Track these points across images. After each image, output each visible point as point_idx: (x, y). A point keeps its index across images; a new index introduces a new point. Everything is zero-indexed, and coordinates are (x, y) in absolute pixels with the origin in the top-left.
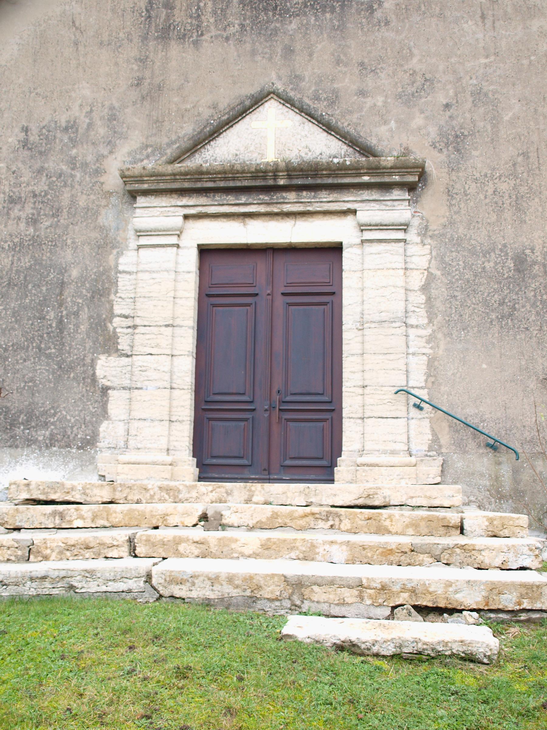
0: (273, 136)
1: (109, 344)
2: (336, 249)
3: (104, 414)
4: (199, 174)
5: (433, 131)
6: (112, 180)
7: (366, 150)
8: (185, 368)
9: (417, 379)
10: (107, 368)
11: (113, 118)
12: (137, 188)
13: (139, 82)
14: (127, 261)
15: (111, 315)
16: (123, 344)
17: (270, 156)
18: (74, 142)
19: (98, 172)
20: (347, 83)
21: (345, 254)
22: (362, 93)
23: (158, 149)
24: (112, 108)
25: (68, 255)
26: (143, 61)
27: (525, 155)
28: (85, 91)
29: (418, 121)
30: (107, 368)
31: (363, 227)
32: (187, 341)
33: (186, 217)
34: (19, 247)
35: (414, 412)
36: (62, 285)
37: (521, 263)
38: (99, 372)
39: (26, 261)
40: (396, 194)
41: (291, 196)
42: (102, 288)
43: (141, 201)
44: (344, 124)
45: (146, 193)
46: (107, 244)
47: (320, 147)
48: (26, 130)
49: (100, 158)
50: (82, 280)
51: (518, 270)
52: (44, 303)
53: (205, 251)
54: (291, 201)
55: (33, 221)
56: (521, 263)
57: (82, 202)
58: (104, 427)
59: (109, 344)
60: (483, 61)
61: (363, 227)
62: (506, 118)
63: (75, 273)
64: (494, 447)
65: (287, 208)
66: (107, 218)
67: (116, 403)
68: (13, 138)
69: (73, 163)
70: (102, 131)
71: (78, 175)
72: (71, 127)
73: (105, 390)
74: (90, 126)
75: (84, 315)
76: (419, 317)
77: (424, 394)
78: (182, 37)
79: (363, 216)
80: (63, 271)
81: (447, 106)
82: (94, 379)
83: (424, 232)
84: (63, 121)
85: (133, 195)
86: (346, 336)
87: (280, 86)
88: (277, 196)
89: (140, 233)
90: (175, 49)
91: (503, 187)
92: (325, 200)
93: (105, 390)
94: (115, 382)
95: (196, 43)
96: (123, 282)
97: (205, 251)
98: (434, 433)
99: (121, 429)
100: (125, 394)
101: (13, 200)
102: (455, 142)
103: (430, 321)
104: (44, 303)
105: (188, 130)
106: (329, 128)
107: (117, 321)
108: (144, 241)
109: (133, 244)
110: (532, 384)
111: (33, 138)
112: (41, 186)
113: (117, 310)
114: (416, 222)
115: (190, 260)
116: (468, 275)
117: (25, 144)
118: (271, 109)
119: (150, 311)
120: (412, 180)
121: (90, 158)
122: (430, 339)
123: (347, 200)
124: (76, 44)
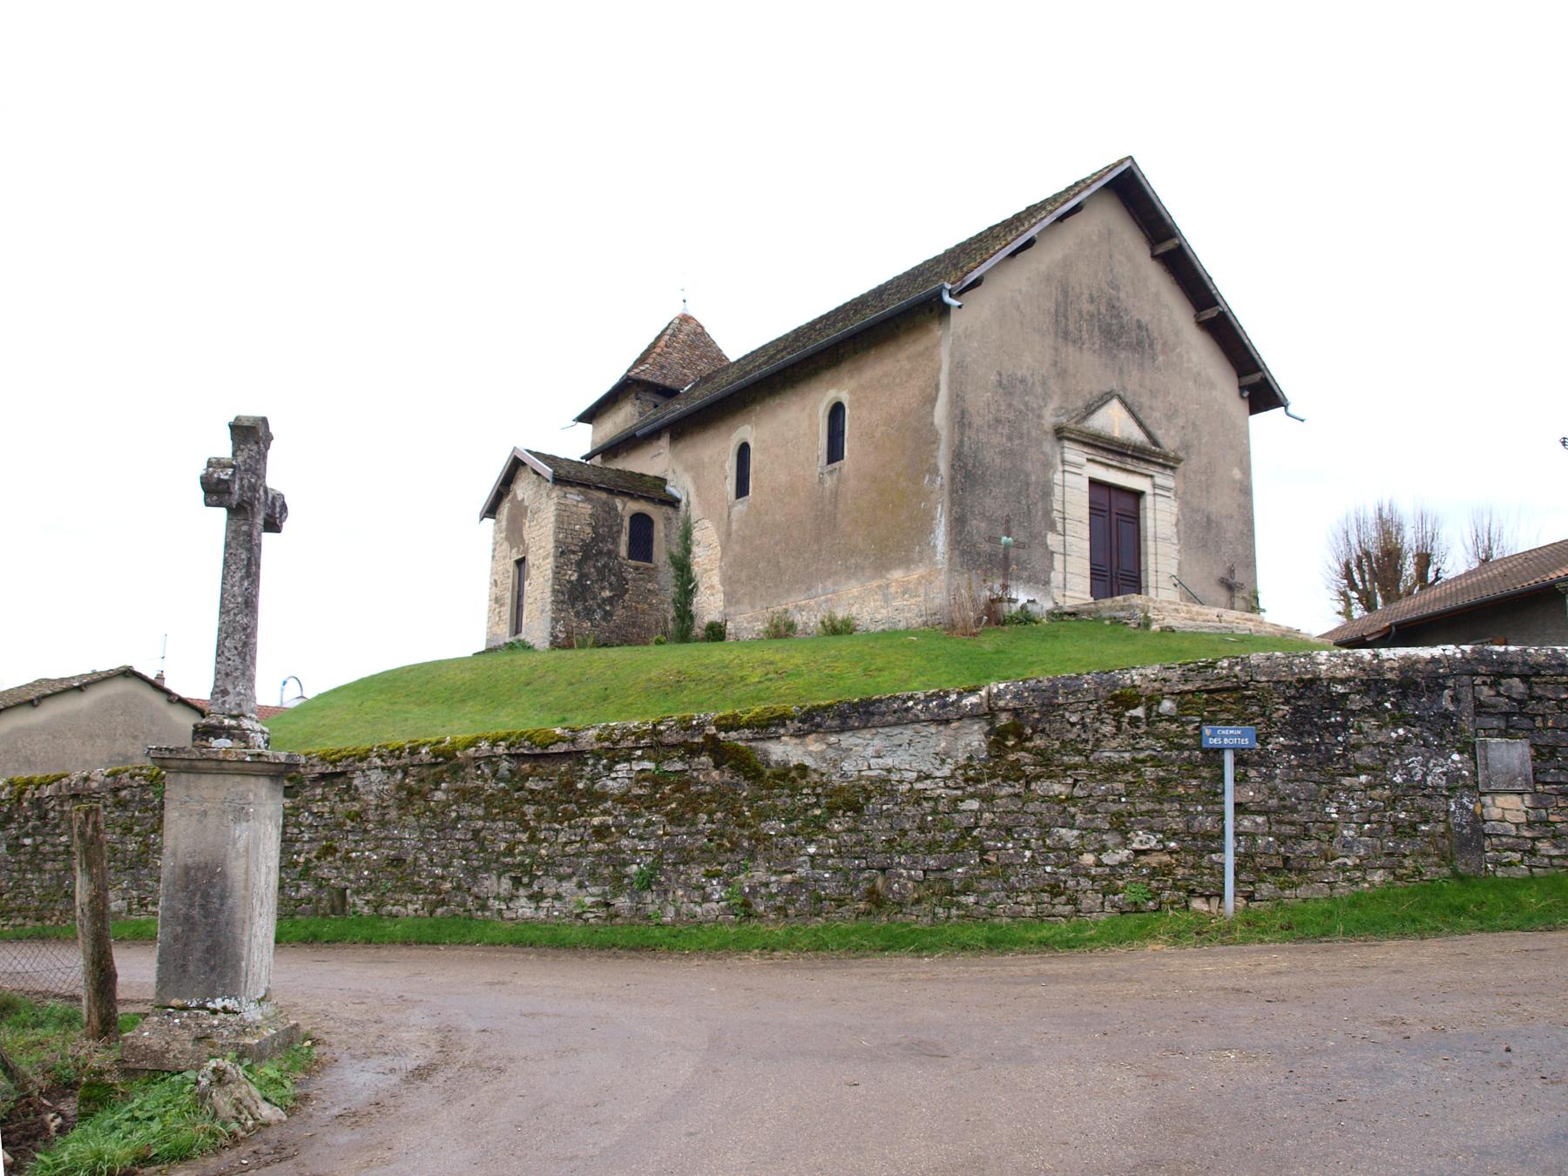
1: (1052, 526)
2: (1138, 495)
7: (1155, 443)
11: (1044, 383)
16: (1059, 527)
18: (1026, 393)
23: (1067, 411)
25: (1029, 467)
26: (1056, 349)
30: (1053, 540)
34: (1003, 453)
39: (1008, 465)
42: (1047, 493)
44: (1147, 423)
45: (1069, 439)
46: (1047, 466)
47: (1138, 436)
48: (1000, 374)
49: (1040, 408)
50: (1037, 483)
54: (1130, 464)
59: (1052, 526)
61: (1155, 486)
67: (1058, 561)
68: (994, 378)
75: (1040, 505)
78: (1074, 342)
80: (1027, 475)
82: (1047, 547)
90: (1071, 349)
92: (1142, 467)
96: (1057, 490)
99: (1061, 577)
101: (998, 421)
106: (1141, 425)
111: (1004, 381)
112: (1012, 417)
113: (1055, 506)
118: (1115, 403)
119: (1071, 511)
123: (1152, 470)
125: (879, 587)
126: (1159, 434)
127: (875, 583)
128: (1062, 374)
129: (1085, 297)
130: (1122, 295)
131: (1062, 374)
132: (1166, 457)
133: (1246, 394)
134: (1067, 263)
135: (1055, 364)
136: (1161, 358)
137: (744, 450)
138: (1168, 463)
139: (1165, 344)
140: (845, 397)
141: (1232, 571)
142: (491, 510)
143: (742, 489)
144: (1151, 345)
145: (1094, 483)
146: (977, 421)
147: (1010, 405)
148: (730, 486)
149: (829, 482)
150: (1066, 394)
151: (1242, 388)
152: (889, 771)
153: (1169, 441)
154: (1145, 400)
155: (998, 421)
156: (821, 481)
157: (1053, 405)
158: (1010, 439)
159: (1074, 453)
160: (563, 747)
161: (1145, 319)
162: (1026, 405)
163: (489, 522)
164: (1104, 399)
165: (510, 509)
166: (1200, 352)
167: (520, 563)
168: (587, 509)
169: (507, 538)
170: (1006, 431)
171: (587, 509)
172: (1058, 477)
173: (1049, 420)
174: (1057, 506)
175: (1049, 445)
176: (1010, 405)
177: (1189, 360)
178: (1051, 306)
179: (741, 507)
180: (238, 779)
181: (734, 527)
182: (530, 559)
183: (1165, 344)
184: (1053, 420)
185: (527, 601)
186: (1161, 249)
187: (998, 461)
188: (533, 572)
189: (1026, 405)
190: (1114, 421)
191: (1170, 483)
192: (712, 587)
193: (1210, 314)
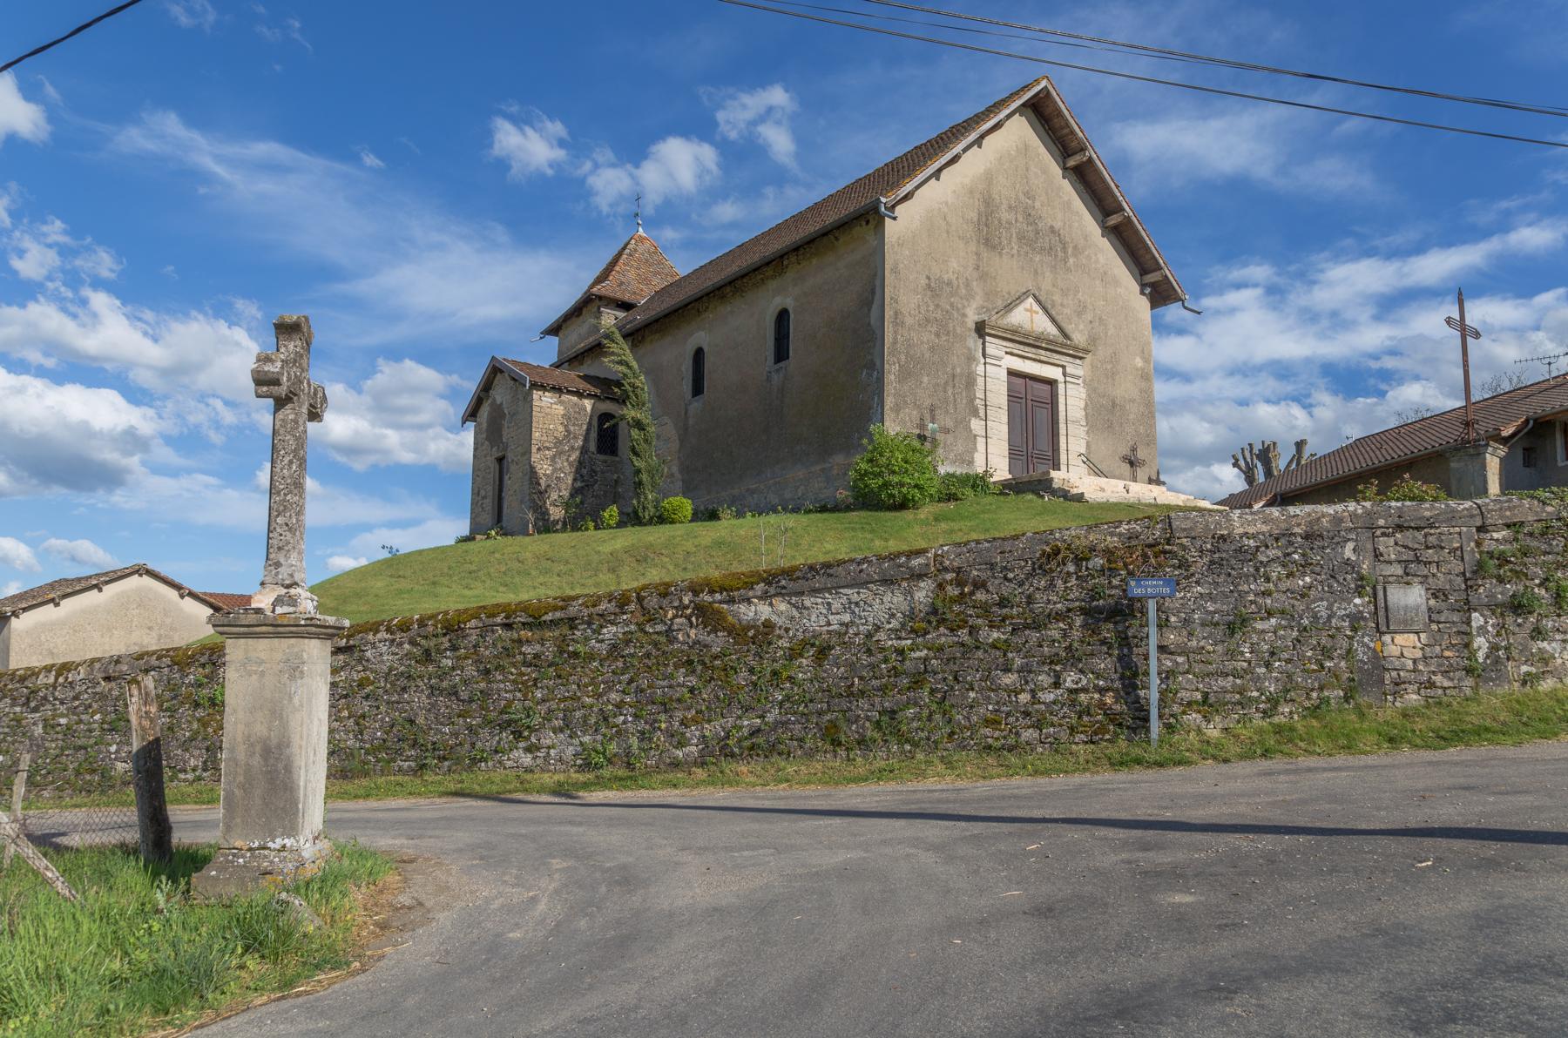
1: (975, 413)
2: (1052, 383)
7: (1066, 336)
11: (967, 285)
16: (982, 413)
18: (952, 294)
30: (976, 425)
42: (970, 382)
46: (971, 359)
59: (975, 413)
61: (1065, 374)
67: (981, 442)
68: (923, 282)
96: (980, 381)
106: (1053, 320)
112: (939, 316)
123: (1063, 360)
125: (823, 470)
126: (1069, 328)
127: (818, 468)
128: (983, 277)
129: (1004, 207)
130: (1037, 204)
131: (983, 277)
132: (1076, 348)
133: (1148, 291)
134: (989, 178)
135: (977, 268)
137: (699, 355)
138: (1078, 354)
139: (1075, 247)
140: (789, 303)
141: (1134, 450)
142: (472, 414)
143: (698, 389)
144: (1064, 249)
145: (1012, 373)
146: (909, 321)
147: (937, 306)
148: (687, 386)
149: (776, 379)
150: (987, 295)
151: (1143, 286)
152: (847, 625)
154: (1057, 298)
155: (928, 321)
156: (769, 379)
158: (938, 335)
159: (994, 347)
160: (558, 615)
161: (1058, 225)
162: (952, 305)
163: (471, 425)
164: (1019, 299)
165: (490, 413)
166: (1106, 254)
167: (500, 460)
168: (560, 409)
169: (487, 439)
170: (934, 329)
171: (560, 409)
172: (980, 369)
173: (972, 317)
174: (980, 394)
175: (973, 342)
176: (937, 306)
177: (1097, 261)
178: (974, 215)
179: (696, 405)
180: (293, 641)
181: (691, 422)
182: (510, 456)
183: (1075, 247)
184: (976, 318)
185: (506, 494)
186: (1071, 163)
187: (927, 355)
188: (513, 468)
189: (952, 305)
190: (1026, 316)
191: (1080, 372)
192: (672, 475)
193: (1114, 220)
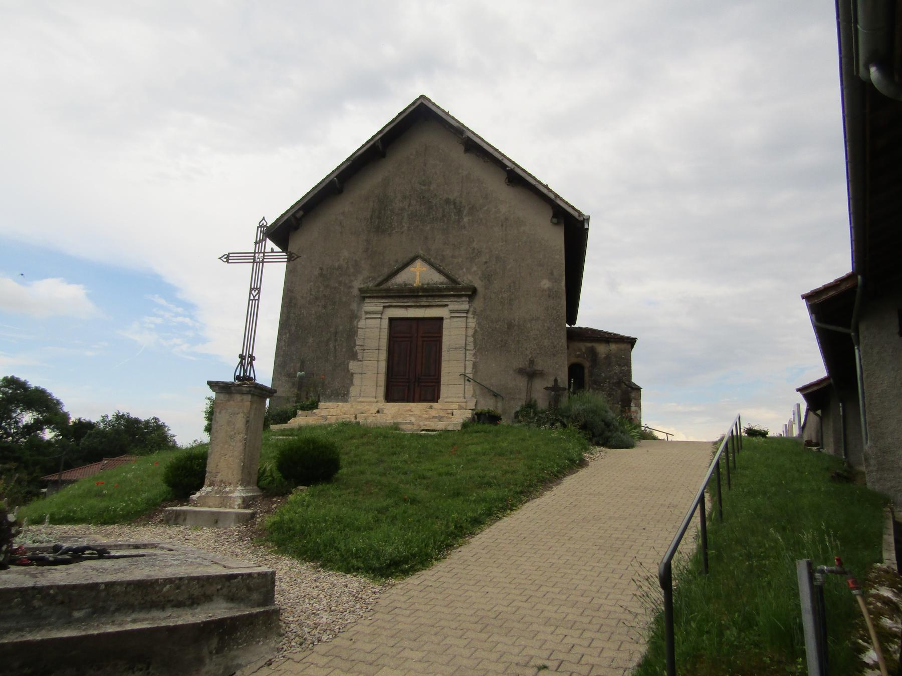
0: (419, 274)
1: (354, 356)
2: (441, 319)
3: (352, 383)
4: (388, 290)
5: (480, 273)
6: (355, 292)
7: (454, 281)
8: (383, 365)
9: (469, 370)
10: (353, 366)
12: (365, 295)
13: (366, 250)
14: (362, 324)
15: (355, 345)
16: (360, 357)
17: (417, 283)
19: (351, 287)
20: (448, 252)
21: (445, 322)
22: (453, 257)
24: (356, 261)
27: (514, 283)
28: (346, 253)
29: (475, 269)
30: (353, 366)
31: (452, 311)
32: (383, 356)
33: (384, 307)
35: (467, 382)
36: (336, 333)
37: (510, 326)
38: (350, 367)
40: (464, 299)
41: (424, 299)
42: (352, 333)
43: (367, 300)
45: (369, 297)
46: (354, 317)
47: (436, 278)
48: (321, 269)
49: (351, 281)
51: (508, 328)
52: (329, 340)
53: (391, 320)
55: (325, 307)
56: (510, 326)
57: (344, 299)
58: (352, 389)
59: (354, 356)
60: (501, 244)
61: (452, 311)
62: (508, 268)
63: (341, 328)
64: (496, 395)
65: (423, 304)
66: (354, 306)
67: (357, 380)
68: (316, 272)
69: (340, 283)
70: (352, 270)
71: (342, 288)
72: (340, 267)
73: (352, 374)
74: (348, 268)
76: (471, 346)
77: (471, 376)
79: (451, 307)
81: (486, 262)
82: (348, 370)
83: (474, 313)
84: (336, 265)
85: (364, 298)
86: (443, 354)
87: (421, 252)
88: (419, 300)
89: (367, 313)
91: (505, 295)
92: (438, 301)
93: (352, 374)
94: (356, 371)
95: (390, 235)
96: (360, 332)
97: (391, 320)
98: (474, 390)
100: (360, 376)
102: (488, 278)
103: (475, 348)
104: (329, 340)
105: (386, 271)
106: (440, 271)
107: (357, 347)
108: (368, 316)
109: (364, 317)
110: (511, 372)
113: (358, 343)
114: (472, 309)
115: (385, 323)
116: (490, 330)
117: (321, 275)
120: (472, 293)
121: (347, 282)
122: (475, 354)
123: (445, 301)
124: (341, 233)
136: (466, 220)
153: (469, 277)
155: (317, 298)
157: (360, 278)
158: (325, 307)
